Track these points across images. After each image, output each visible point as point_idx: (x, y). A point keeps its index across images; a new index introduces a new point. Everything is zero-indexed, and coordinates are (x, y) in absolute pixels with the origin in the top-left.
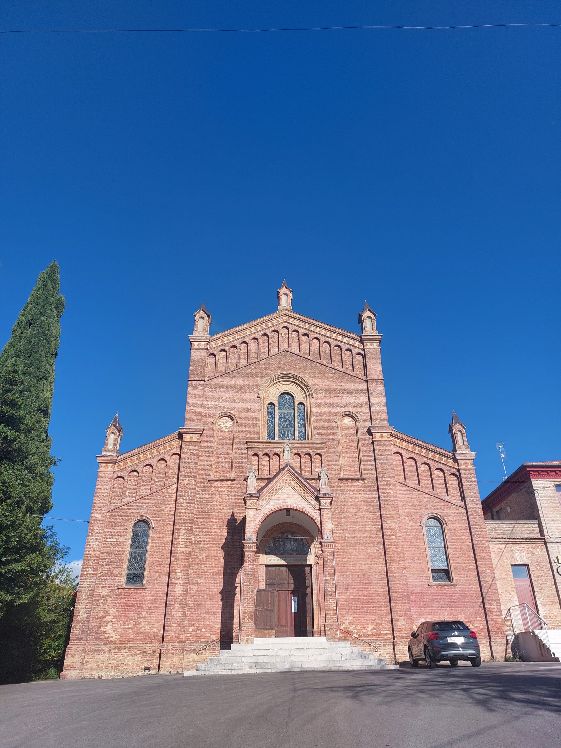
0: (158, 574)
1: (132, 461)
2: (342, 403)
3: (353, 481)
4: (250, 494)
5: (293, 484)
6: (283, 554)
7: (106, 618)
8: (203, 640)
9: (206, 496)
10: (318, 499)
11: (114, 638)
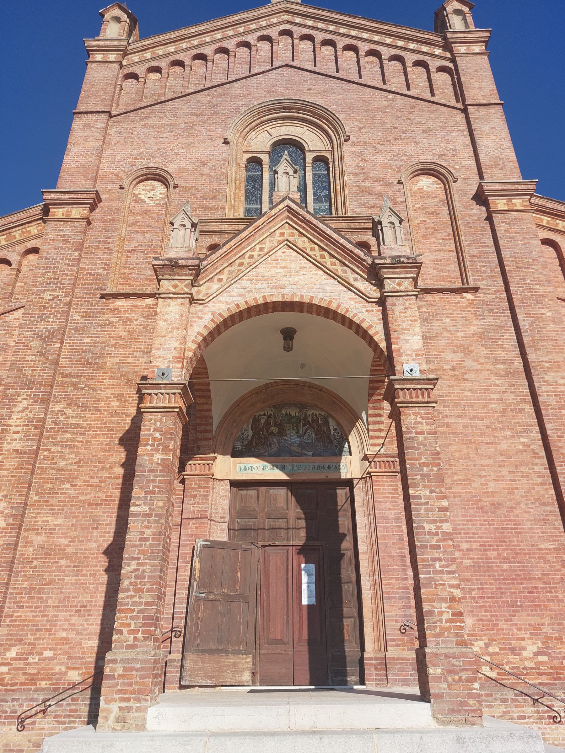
2: (411, 149)
3: (449, 296)
4: (170, 260)
5: (302, 242)
6: (277, 455)
8: (43, 684)
9: (92, 328)
10: (375, 275)
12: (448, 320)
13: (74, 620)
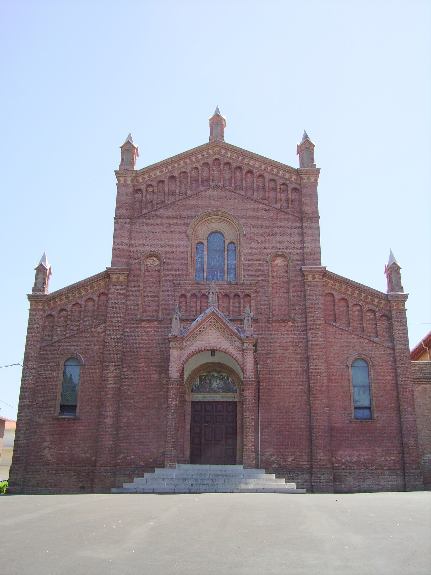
0: (89, 407)
1: (61, 300)
7: (44, 444)
11: (51, 461)
12: (280, 335)
13: (140, 447)
